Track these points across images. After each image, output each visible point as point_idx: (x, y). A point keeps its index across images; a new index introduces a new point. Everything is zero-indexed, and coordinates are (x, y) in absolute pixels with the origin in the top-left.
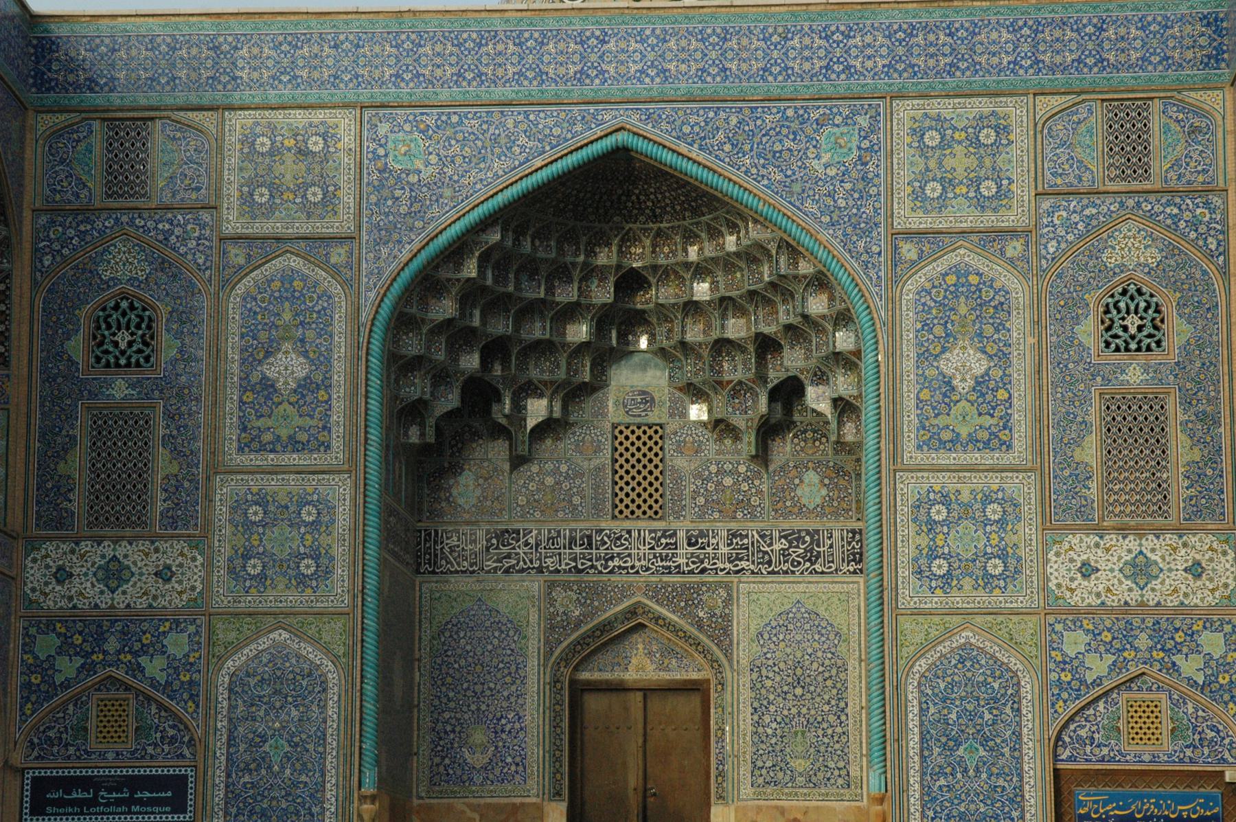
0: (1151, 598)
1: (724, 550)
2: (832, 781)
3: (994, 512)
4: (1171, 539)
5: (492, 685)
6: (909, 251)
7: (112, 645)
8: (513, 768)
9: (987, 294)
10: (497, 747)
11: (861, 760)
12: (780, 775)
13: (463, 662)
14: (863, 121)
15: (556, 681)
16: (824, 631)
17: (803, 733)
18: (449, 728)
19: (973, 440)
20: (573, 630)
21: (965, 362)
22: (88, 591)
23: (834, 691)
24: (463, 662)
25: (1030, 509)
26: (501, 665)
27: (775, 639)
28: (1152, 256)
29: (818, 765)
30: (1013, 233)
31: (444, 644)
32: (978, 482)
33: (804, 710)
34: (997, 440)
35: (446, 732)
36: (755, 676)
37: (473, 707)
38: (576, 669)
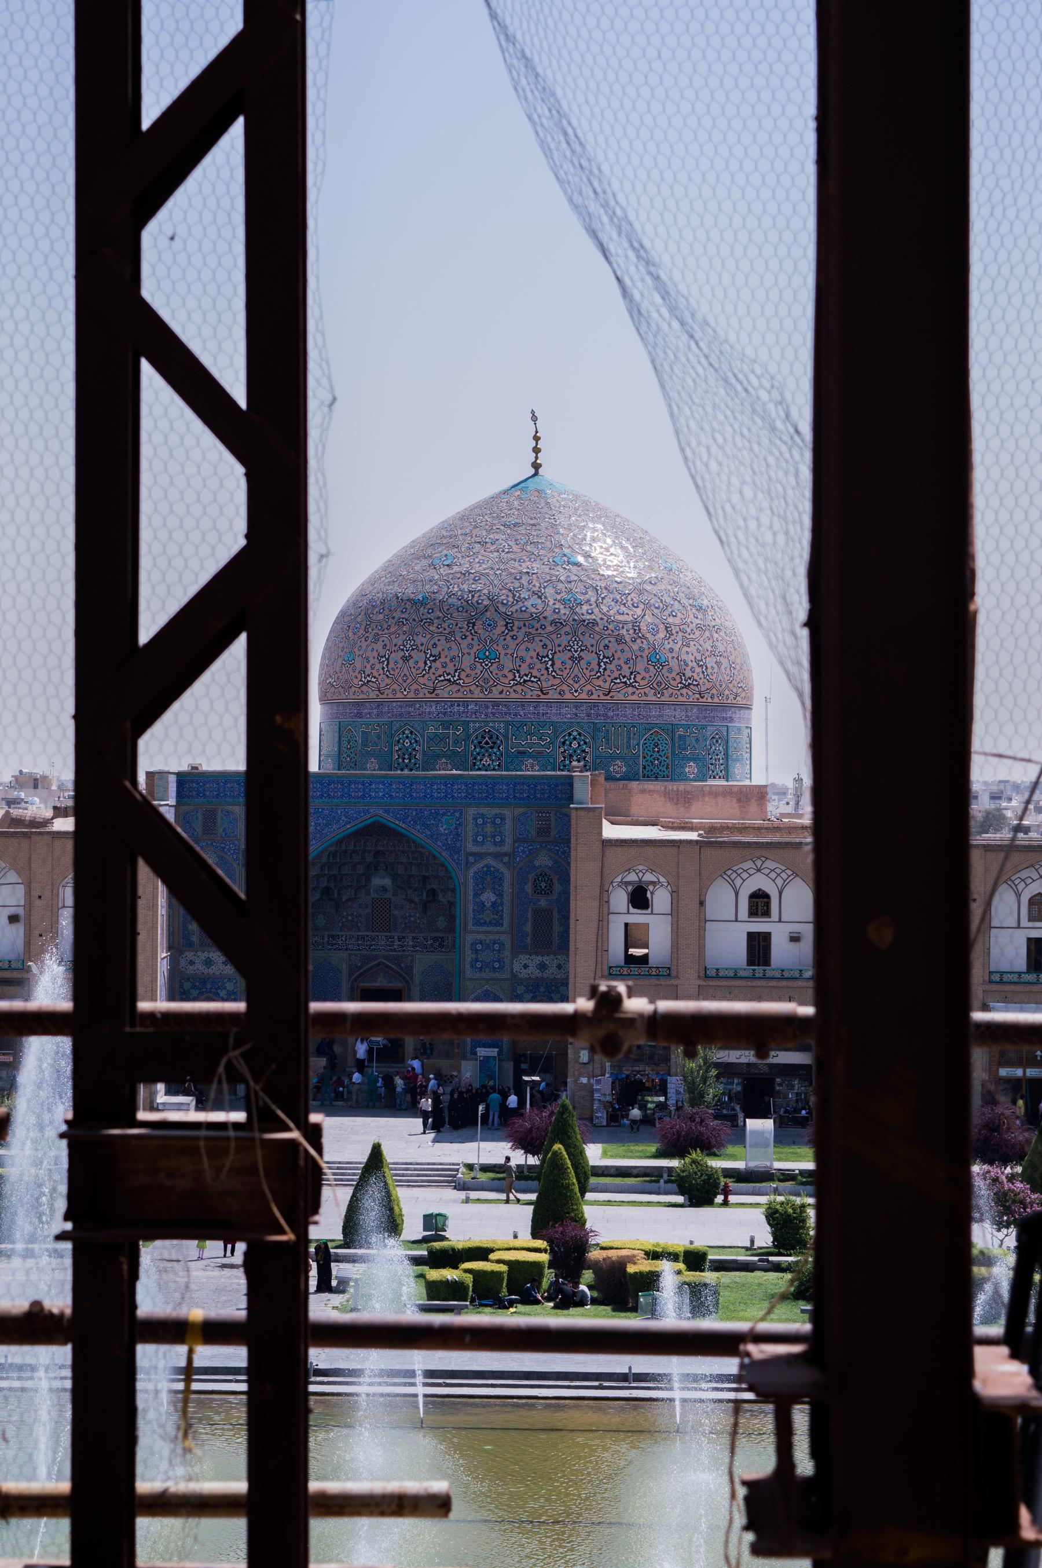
0: (545, 975)
1: (411, 943)
3: (496, 947)
4: (552, 956)
6: (471, 859)
7: (209, 986)
9: (497, 874)
14: (457, 815)
15: (352, 987)
19: (491, 923)
21: (488, 897)
22: (199, 968)
25: (508, 945)
28: (550, 863)
30: (505, 854)
32: (492, 937)
34: (498, 923)
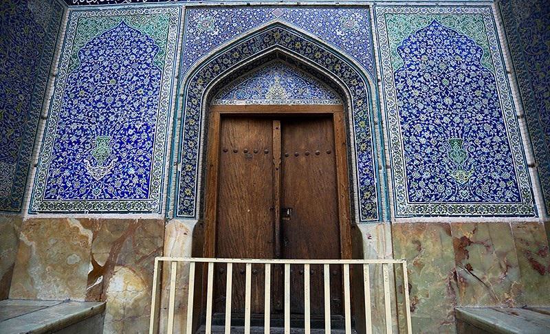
2: (500, 194)
5: (124, 97)
8: (135, 180)
10: (120, 159)
11: (528, 171)
12: (441, 187)
13: (98, 77)
16: (464, 47)
17: (460, 143)
18: (74, 139)
20: (211, 48)
23: (485, 101)
24: (98, 77)
26: (135, 78)
27: (416, 53)
29: (480, 176)
31: (83, 61)
33: (457, 120)
35: (70, 143)
36: (400, 86)
37: (102, 119)
38: (215, 93)
